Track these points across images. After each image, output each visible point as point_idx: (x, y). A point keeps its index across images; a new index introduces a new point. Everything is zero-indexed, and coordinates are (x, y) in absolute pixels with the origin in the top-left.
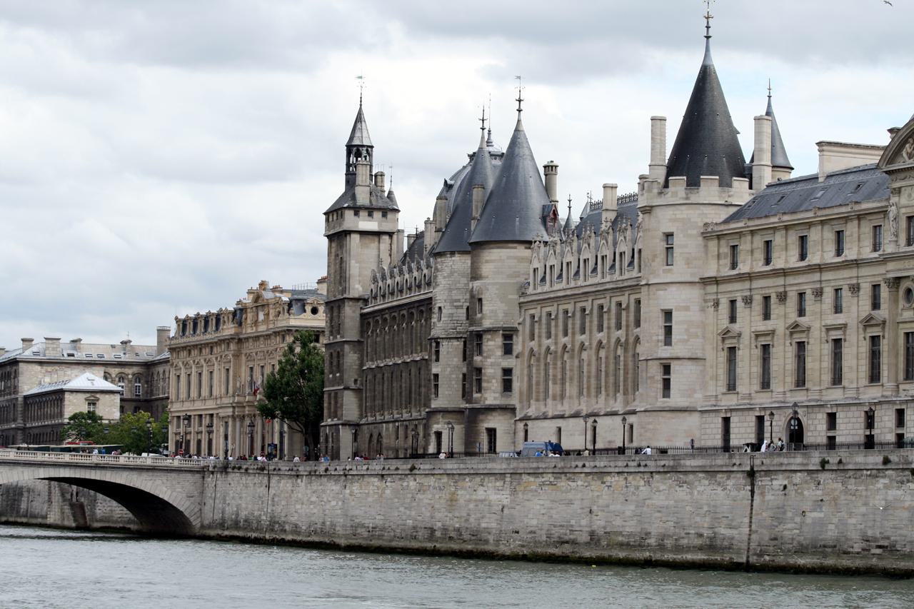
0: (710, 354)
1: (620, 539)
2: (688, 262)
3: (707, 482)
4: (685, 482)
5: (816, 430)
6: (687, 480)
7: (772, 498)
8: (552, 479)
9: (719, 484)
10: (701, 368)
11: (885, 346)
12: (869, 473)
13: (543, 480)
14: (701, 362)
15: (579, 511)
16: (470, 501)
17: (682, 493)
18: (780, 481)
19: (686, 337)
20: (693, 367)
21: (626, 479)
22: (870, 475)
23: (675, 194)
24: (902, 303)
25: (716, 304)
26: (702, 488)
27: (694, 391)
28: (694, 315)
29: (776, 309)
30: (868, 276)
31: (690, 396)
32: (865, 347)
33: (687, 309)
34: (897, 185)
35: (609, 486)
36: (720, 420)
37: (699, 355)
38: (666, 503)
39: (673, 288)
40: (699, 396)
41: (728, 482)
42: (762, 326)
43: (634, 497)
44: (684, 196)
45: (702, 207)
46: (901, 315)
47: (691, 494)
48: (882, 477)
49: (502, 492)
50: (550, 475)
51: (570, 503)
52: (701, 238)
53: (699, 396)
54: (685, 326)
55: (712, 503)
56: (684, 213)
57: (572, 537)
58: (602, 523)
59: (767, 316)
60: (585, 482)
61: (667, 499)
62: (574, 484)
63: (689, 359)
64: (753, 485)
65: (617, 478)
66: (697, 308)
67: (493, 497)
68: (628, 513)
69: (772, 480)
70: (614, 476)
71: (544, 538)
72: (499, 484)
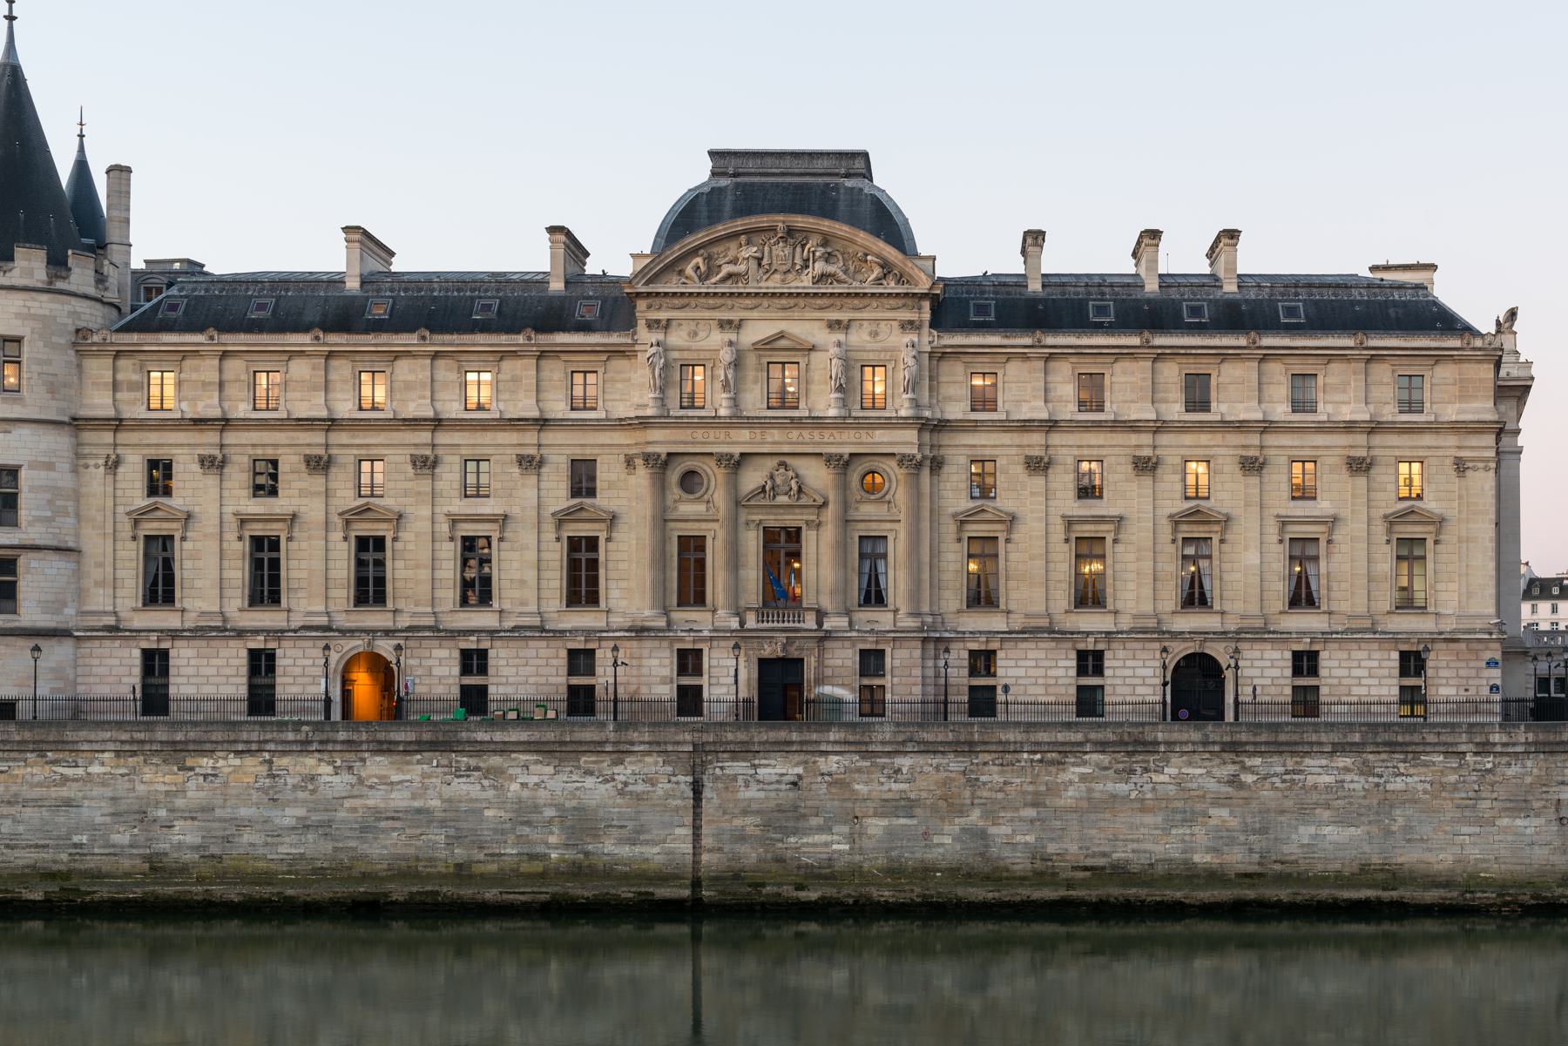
0: (94, 544)
2: (52, 389)
3: (550, 770)
4: (477, 769)
6: (482, 765)
7: (762, 795)
9: (588, 773)
10: (73, 566)
12: (1038, 756)
14: (74, 556)
17: (466, 788)
18: (776, 768)
19: (49, 514)
20: (62, 564)
21: (270, 762)
22: (1041, 761)
23: (31, 273)
24: (675, 492)
25: (114, 465)
26: (536, 779)
27: (65, 604)
28: (62, 478)
30: (561, 448)
31: (58, 612)
32: (556, 555)
33: (50, 466)
34: (663, 315)
35: (205, 776)
36: (137, 653)
37: (71, 545)
38: (417, 804)
39: (25, 431)
40: (70, 611)
41: (617, 770)
43: (301, 795)
44: (45, 278)
45: (73, 300)
46: (675, 509)
48: (1074, 765)
52: (72, 353)
53: (70, 611)
54: (48, 496)
55: (569, 804)
56: (44, 305)
58: (192, 839)
60: (118, 767)
61: (414, 797)
62: (80, 771)
63: (57, 549)
65: (237, 762)
66: (67, 466)
69: (755, 766)
70: (226, 758)
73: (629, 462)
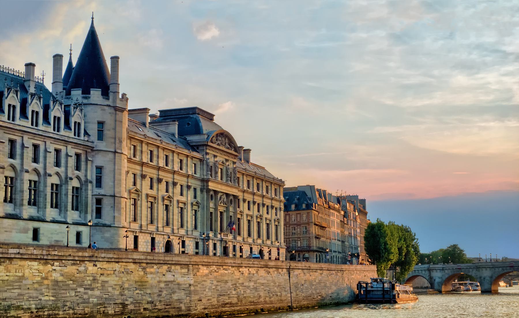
1: (250, 299)
5: (177, 247)
8: (216, 269)
11: (199, 214)
13: (211, 269)
15: (231, 286)
16: (159, 282)
17: (269, 277)
29: (155, 185)
42: (150, 192)
47: (272, 277)
49: (187, 276)
50: (214, 267)
51: (226, 282)
57: (230, 301)
59: (151, 188)
64: (289, 274)
67: (180, 279)
68: (252, 287)
71: (216, 303)
72: (185, 271)
73: (202, 191)
